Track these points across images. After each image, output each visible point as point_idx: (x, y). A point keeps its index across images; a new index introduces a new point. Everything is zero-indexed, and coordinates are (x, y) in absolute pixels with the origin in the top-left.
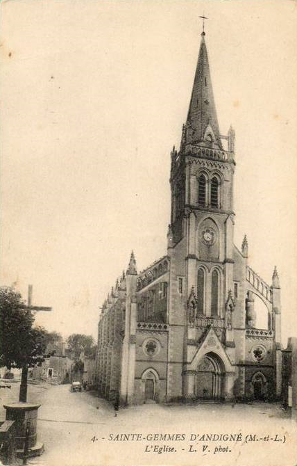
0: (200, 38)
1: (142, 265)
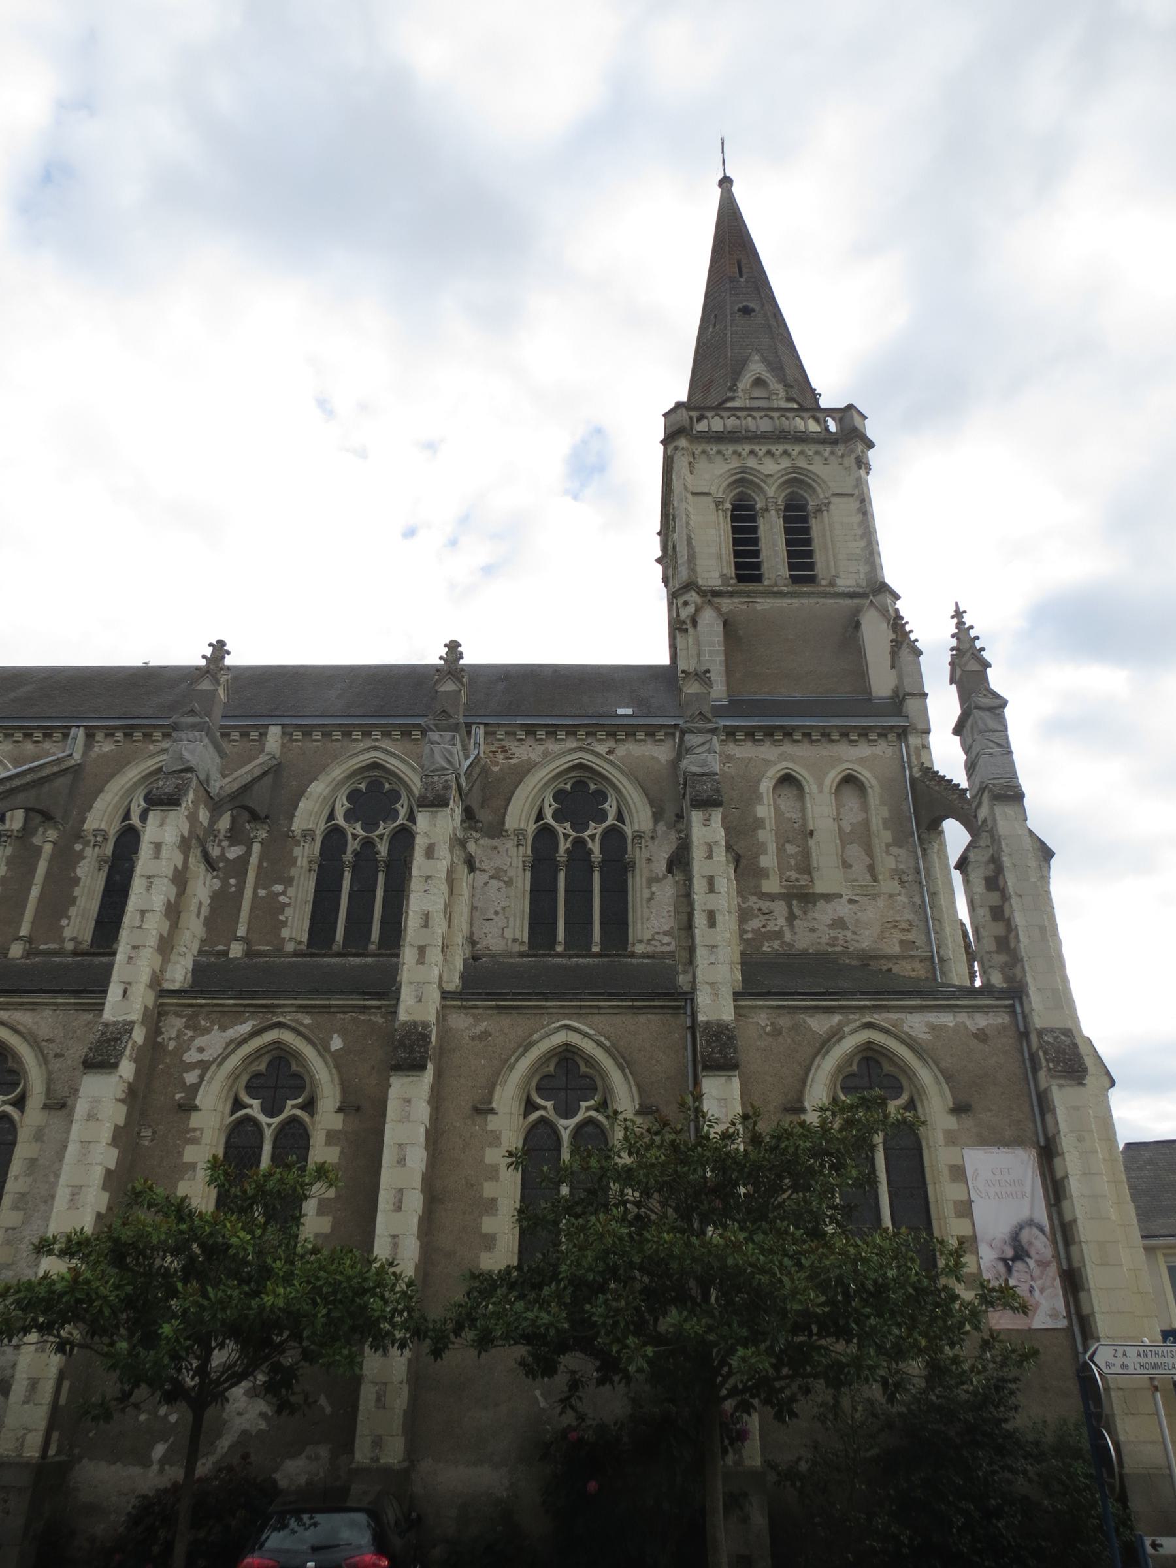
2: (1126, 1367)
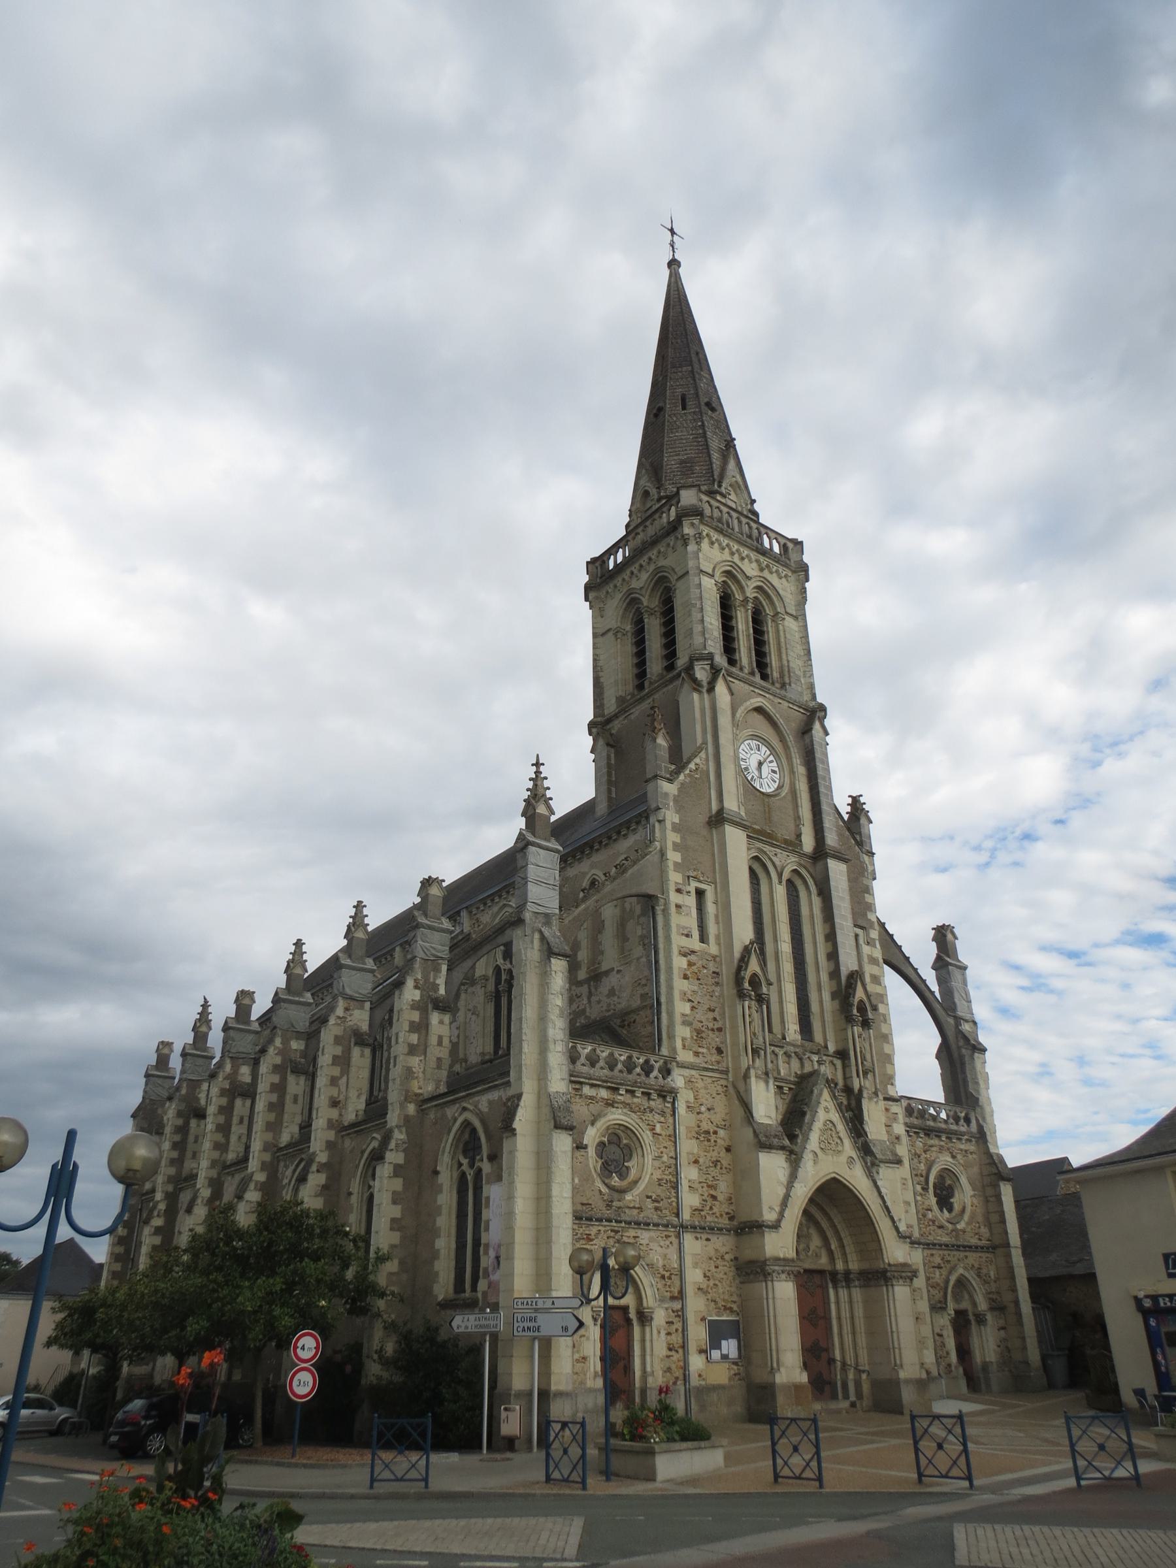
0: (666, 273)
2: (467, 1327)
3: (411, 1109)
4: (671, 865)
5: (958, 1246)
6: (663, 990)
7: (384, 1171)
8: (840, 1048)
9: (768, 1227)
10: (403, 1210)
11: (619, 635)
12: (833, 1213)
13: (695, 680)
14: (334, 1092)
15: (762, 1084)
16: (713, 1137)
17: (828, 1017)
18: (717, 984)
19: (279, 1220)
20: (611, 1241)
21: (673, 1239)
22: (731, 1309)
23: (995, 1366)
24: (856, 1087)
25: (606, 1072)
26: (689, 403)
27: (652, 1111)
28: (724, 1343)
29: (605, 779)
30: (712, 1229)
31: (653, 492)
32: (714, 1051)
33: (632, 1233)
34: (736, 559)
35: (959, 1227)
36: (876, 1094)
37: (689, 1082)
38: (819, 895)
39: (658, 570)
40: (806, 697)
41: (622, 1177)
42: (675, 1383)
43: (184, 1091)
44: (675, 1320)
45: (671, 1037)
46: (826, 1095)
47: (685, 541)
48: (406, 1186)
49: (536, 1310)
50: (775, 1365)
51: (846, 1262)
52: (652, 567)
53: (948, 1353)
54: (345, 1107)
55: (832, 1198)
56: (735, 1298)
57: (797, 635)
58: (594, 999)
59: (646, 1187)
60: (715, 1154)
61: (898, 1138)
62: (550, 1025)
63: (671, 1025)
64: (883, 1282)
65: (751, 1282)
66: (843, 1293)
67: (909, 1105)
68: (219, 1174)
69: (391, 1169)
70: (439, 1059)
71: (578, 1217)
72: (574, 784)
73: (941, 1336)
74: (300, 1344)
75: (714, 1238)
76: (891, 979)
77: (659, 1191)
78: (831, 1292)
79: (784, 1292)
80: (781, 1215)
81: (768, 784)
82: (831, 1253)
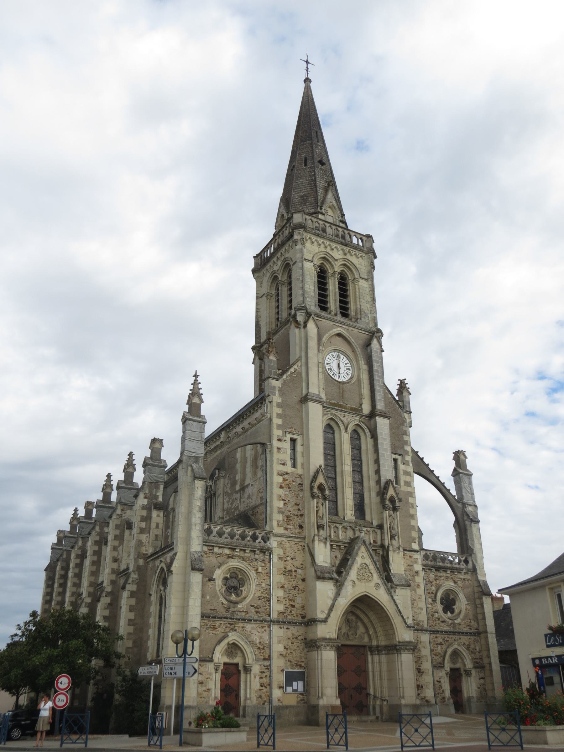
0: (303, 85)
1: (217, 412)
3: (141, 562)
4: (275, 426)
5: (455, 632)
6: (268, 495)
7: (125, 594)
8: (380, 523)
9: (319, 621)
10: (135, 615)
11: (269, 297)
12: (371, 614)
13: (296, 322)
14: (115, 554)
15: (322, 545)
16: (294, 574)
17: (374, 507)
18: (302, 490)
19: (73, 621)
20: (228, 629)
21: (266, 628)
22: (301, 666)
23: (475, 699)
24: (387, 544)
25: (229, 540)
26: (309, 162)
27: (256, 560)
28: (295, 683)
29: (258, 378)
30: (289, 623)
31: (285, 215)
32: (298, 527)
33: (241, 625)
34: (328, 250)
35: (456, 621)
36: (399, 548)
37: (280, 544)
38: (372, 437)
39: (286, 260)
40: (371, 325)
41: (237, 595)
42: (264, 704)
43: (65, 556)
44: (265, 671)
45: (271, 520)
46: (363, 549)
47: (296, 243)
48: (137, 602)
49: (176, 664)
50: (320, 695)
51: (378, 641)
52: (283, 258)
53: (443, 691)
54: (121, 562)
55: (364, 605)
56: (303, 660)
57: (367, 290)
58: (242, 500)
59: (251, 600)
60: (295, 582)
61: (417, 573)
62: (193, 516)
63: (271, 514)
64: (395, 652)
65: (311, 651)
66: (376, 658)
67: (426, 554)
68: (76, 599)
69: (129, 593)
70: (157, 536)
71: (203, 616)
72: (231, 382)
73: (440, 682)
74: (60, 681)
75: (291, 628)
76: (419, 482)
77: (259, 602)
78: (370, 657)
79: (328, 658)
80: (329, 615)
81: (344, 377)
82: (369, 636)
